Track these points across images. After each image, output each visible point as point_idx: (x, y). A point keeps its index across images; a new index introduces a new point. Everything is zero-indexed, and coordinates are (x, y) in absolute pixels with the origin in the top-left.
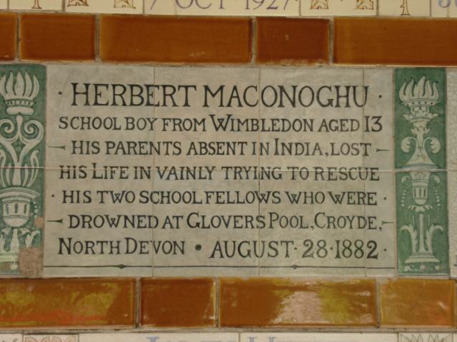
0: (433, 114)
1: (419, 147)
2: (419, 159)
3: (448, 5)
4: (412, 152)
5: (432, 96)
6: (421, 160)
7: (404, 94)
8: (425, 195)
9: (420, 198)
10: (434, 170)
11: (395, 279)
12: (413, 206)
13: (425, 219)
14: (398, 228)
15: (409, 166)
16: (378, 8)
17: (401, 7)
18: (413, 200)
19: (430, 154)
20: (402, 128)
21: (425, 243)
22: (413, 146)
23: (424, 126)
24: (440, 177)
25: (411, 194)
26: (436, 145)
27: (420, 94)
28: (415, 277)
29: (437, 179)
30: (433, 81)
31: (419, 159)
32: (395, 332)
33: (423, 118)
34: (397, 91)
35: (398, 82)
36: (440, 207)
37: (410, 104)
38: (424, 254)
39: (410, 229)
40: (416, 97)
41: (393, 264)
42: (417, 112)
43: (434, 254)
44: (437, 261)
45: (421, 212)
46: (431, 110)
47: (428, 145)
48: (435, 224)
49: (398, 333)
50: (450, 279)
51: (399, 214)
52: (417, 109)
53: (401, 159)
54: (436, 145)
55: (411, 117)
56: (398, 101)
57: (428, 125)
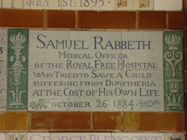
0: (23, 47)
1: (18, 60)
2: (17, 64)
3: (30, 4)
4: (14, 62)
5: (23, 40)
6: (18, 65)
7: (12, 39)
8: (19, 79)
9: (17, 80)
10: (23, 69)
11: (5, 112)
12: (14, 83)
13: (19, 88)
14: (8, 91)
15: (14, 67)
16: (2, 5)
17: (11, 4)
18: (14, 80)
19: (22, 63)
20: (11, 52)
21: (18, 97)
22: (15, 59)
23: (19, 51)
24: (25, 72)
25: (13, 78)
26: (24, 59)
27: (18, 39)
28: (13, 111)
29: (24, 72)
30: (23, 33)
31: (17, 64)
32: (5, 133)
33: (19, 48)
34: (9, 38)
35: (10, 34)
36: (25, 83)
37: (14, 43)
38: (18, 102)
39: (13, 92)
40: (16, 40)
41: (5, 105)
42: (17, 46)
43: (22, 102)
44: (23, 104)
45: (17, 85)
46: (22, 45)
47: (21, 59)
48: (23, 90)
49: (6, 133)
50: (28, 111)
51: (8, 86)
52: (17, 45)
53: (10, 64)
54: (24, 59)
55: (14, 48)
56: (9, 42)
57: (21, 51)
